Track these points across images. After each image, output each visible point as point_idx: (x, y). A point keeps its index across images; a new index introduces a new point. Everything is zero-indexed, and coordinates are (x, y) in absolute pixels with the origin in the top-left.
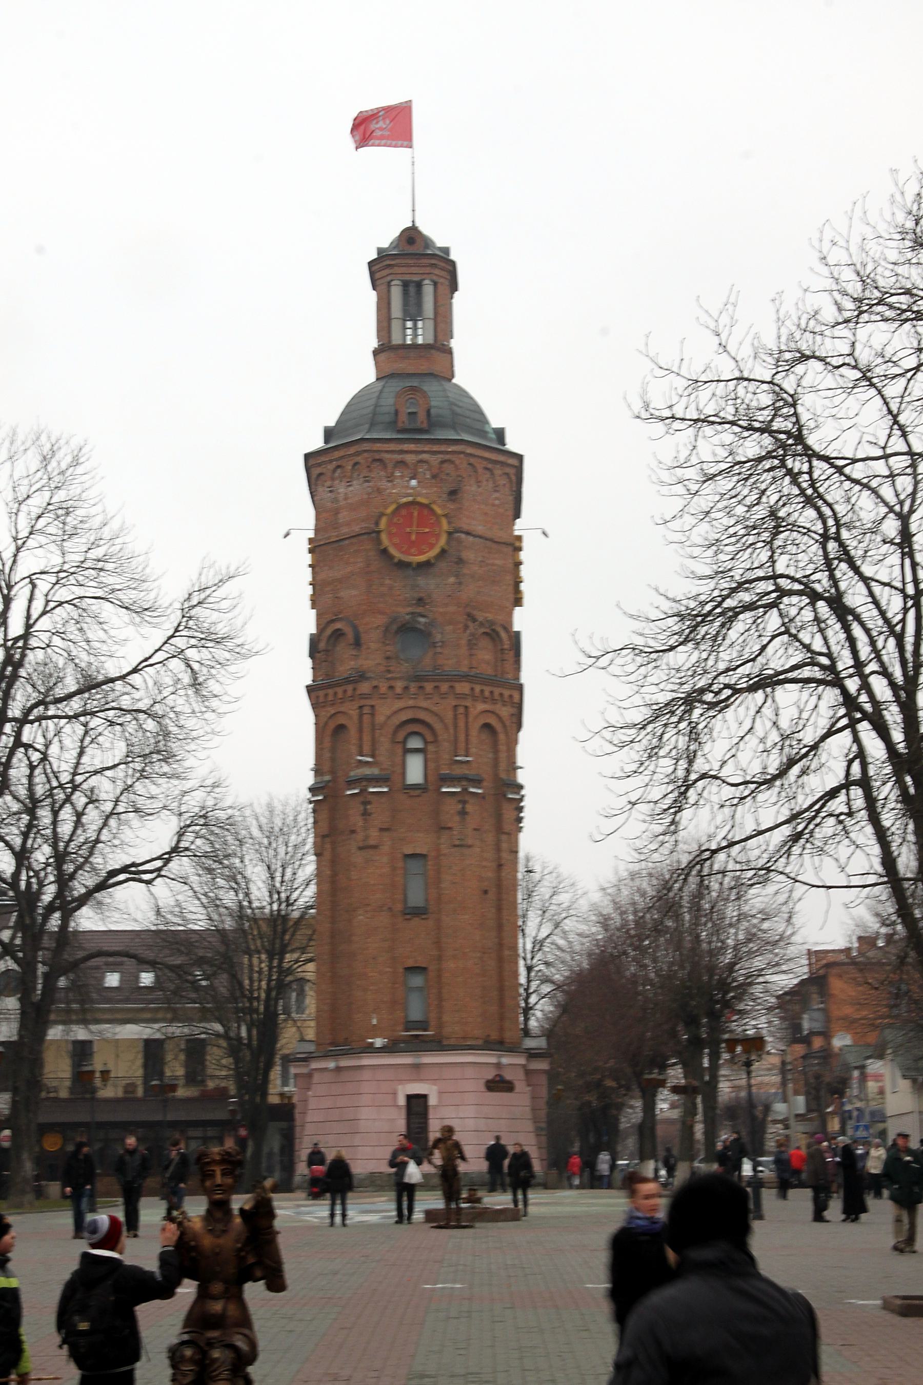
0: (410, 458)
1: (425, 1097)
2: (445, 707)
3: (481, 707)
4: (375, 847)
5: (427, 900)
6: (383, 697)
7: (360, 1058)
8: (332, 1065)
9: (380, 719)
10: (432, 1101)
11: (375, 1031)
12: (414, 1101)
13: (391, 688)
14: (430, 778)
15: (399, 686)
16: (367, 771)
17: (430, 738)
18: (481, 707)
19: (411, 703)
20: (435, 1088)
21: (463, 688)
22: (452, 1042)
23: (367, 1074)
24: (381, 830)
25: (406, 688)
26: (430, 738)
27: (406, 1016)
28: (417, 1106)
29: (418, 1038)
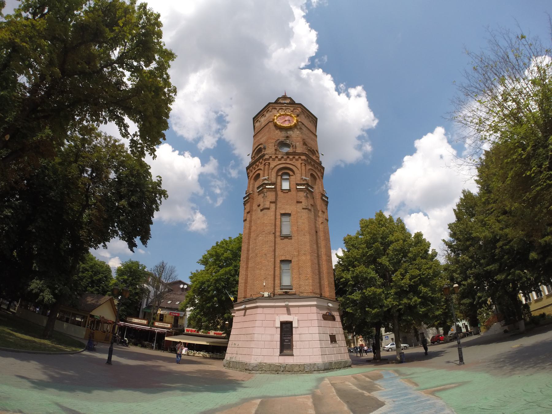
0: (284, 108)
1: (291, 323)
2: (298, 163)
3: (310, 167)
4: (268, 209)
5: (291, 232)
6: (274, 160)
7: (257, 302)
8: (243, 307)
9: (272, 166)
10: (295, 325)
11: (265, 288)
12: (284, 326)
13: (277, 157)
14: (292, 187)
15: (279, 157)
16: (266, 182)
17: (291, 173)
18: (310, 167)
19: (284, 162)
20: (296, 318)
21: (303, 157)
22: (305, 295)
23: (259, 310)
24: (271, 202)
25: (282, 157)
26: (291, 173)
27: (280, 283)
28: (286, 329)
29: (287, 294)
